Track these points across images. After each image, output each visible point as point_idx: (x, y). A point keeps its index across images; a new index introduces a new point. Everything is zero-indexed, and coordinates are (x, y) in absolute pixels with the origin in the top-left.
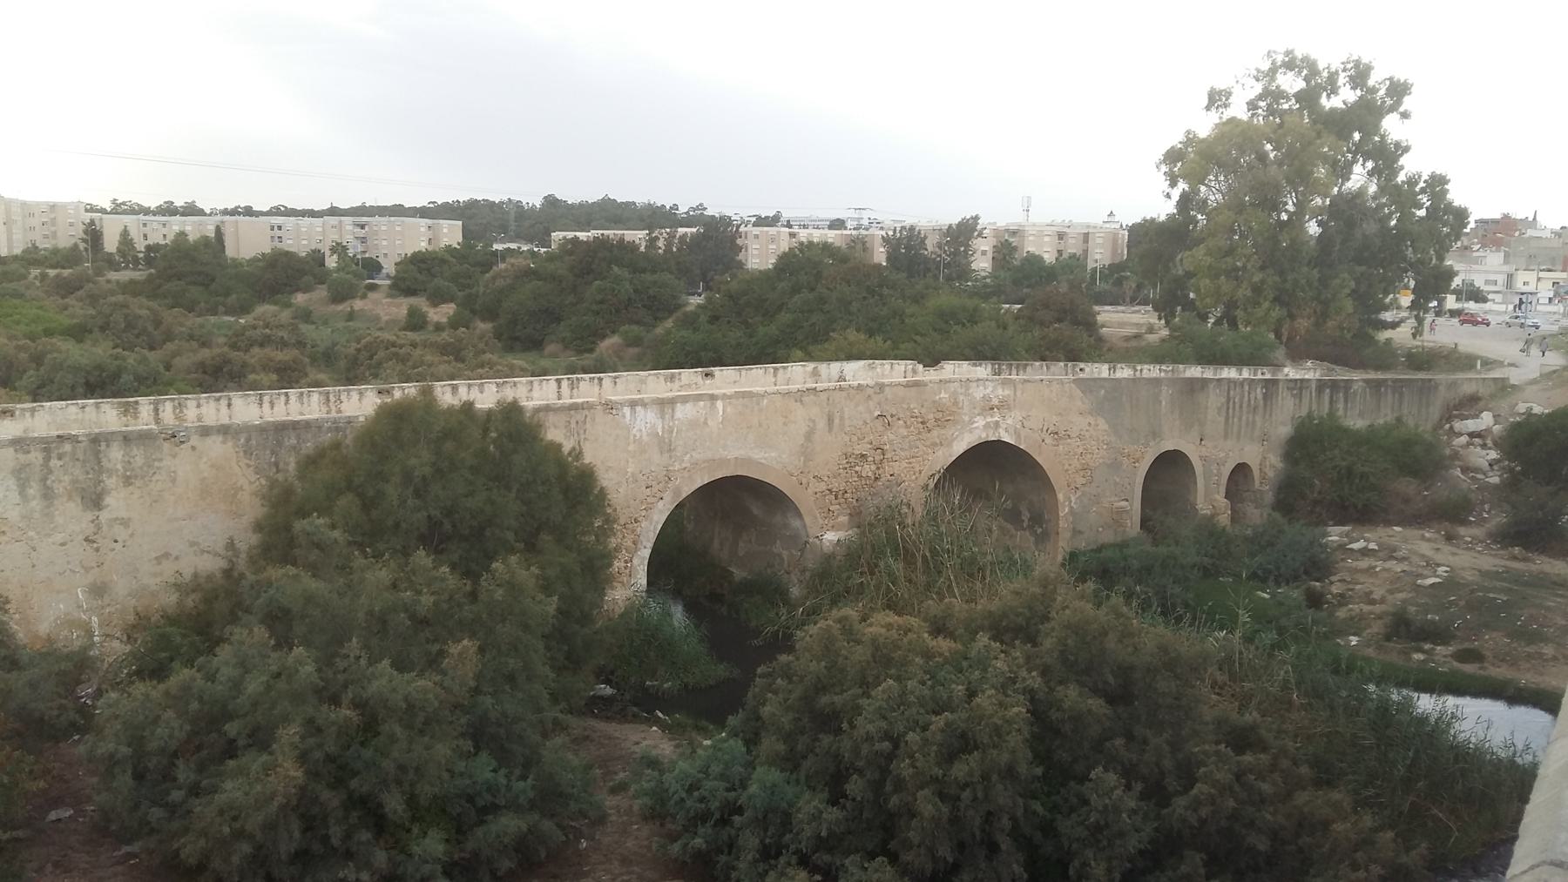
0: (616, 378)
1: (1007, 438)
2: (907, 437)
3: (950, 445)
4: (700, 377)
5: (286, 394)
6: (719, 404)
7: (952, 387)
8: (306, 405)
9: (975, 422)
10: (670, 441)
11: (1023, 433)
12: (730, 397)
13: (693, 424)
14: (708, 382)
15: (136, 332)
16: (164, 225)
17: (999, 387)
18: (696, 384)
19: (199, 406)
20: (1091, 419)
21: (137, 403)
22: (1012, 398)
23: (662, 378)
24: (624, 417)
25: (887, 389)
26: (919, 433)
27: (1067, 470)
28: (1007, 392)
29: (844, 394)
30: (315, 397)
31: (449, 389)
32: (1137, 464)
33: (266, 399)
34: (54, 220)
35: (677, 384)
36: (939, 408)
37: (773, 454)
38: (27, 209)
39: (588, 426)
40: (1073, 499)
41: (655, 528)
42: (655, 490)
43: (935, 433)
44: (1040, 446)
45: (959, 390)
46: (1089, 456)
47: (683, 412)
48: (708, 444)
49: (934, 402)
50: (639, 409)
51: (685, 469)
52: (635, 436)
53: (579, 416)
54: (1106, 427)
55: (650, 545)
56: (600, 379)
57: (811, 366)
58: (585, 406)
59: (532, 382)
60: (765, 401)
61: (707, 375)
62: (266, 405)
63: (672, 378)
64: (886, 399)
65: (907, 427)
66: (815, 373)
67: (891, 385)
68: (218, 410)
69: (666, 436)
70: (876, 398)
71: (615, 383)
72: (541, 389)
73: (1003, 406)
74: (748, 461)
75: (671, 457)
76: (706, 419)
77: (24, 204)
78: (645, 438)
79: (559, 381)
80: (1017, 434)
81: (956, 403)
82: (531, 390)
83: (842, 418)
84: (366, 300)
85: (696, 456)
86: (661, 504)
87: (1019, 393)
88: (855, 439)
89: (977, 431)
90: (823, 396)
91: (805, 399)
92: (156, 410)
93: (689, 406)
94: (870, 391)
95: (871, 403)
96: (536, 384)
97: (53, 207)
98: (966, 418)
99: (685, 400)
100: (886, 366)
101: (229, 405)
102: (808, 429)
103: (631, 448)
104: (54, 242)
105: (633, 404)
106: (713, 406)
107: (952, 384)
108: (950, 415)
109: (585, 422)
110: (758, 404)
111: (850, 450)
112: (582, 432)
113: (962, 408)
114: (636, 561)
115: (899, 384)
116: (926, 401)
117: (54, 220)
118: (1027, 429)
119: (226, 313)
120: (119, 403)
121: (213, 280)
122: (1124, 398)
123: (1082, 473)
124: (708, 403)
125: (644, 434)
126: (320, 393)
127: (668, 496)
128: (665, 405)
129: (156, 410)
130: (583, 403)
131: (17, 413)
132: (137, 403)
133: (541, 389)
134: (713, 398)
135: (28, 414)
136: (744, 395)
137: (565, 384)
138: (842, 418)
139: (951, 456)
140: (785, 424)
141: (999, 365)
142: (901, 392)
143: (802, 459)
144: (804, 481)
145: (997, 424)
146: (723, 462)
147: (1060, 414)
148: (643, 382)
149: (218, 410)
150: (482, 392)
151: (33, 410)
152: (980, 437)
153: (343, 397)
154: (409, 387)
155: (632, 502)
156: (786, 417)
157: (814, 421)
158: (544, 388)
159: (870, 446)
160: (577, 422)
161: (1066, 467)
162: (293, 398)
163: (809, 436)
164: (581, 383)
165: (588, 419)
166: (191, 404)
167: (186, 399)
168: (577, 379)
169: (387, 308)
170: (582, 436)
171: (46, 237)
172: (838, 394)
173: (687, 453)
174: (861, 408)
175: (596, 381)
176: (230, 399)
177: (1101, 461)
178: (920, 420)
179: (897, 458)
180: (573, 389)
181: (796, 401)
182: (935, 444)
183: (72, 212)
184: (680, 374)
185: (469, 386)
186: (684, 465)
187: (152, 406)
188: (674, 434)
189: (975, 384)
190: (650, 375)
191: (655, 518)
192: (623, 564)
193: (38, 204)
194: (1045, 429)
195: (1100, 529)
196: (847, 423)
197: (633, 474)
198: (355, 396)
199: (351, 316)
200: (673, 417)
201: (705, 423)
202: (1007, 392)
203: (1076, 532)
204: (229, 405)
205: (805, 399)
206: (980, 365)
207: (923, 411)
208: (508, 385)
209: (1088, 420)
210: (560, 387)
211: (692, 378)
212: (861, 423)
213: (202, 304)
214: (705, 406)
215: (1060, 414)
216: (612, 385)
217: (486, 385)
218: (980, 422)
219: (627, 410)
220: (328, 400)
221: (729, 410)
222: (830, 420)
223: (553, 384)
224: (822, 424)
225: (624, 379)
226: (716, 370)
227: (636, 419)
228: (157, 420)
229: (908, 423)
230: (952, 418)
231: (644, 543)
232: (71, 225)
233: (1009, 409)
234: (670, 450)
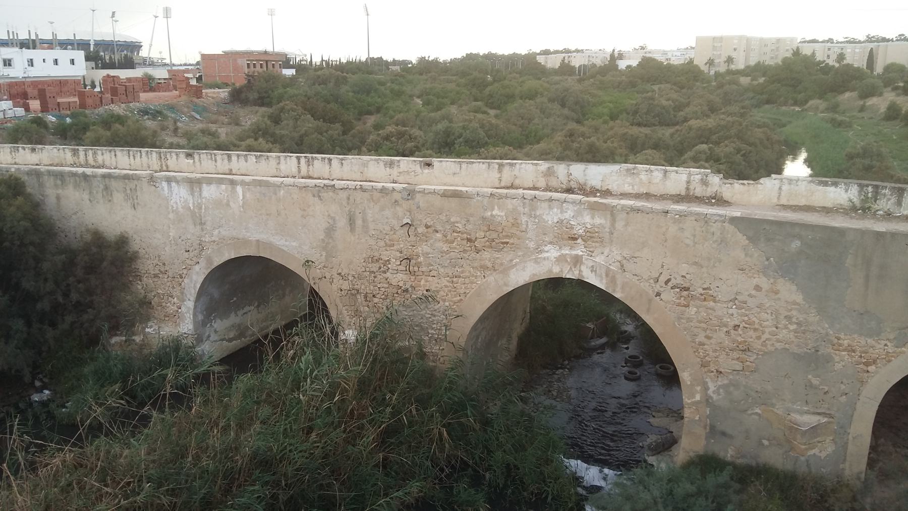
0: (342, 159)
1: (592, 279)
2: (447, 252)
3: (505, 271)
4: (418, 166)
5: (141, 152)
6: (239, 189)
7: (510, 204)
8: (150, 159)
9: (541, 252)
10: (200, 215)
11: (619, 280)
12: (248, 184)
13: (219, 204)
14: (427, 171)
15: (653, 115)
16: (842, 49)
17: (585, 213)
18: (414, 171)
19: (102, 154)
20: (764, 283)
21: (78, 149)
22: (607, 230)
23: (382, 164)
24: (163, 189)
25: (418, 196)
26: (465, 251)
27: (702, 344)
28: (598, 221)
29: (366, 195)
30: (154, 155)
31: (226, 157)
32: (872, 368)
33: (131, 153)
34: (777, 48)
35: (395, 172)
36: (489, 225)
37: (294, 244)
38: (763, 43)
39: (139, 193)
40: (712, 387)
41: (195, 286)
42: (192, 254)
43: (486, 255)
44: (650, 301)
45: (521, 209)
46: (751, 333)
47: (210, 192)
48: (232, 223)
49: (484, 219)
50: (173, 184)
51: (214, 241)
52: (173, 207)
53: (132, 185)
54: (799, 298)
55: (193, 298)
56: (330, 160)
57: (543, 165)
58: (134, 178)
59: (279, 157)
60: (282, 192)
61: (429, 165)
62: (132, 157)
63: (391, 165)
64: (418, 207)
65: (447, 241)
66: (549, 173)
67: (423, 192)
68: (111, 158)
69: (196, 211)
70: (405, 205)
71: (342, 164)
72: (286, 163)
73: (591, 237)
74: (270, 246)
75: (202, 230)
76: (228, 201)
77: (761, 40)
78: (180, 209)
79: (298, 158)
80: (613, 280)
81: (516, 224)
82: (279, 163)
83: (364, 221)
84: (879, 98)
85: (224, 233)
86: (197, 268)
87: (619, 225)
88: (382, 243)
89: (546, 263)
90: (343, 195)
91: (324, 195)
92: (86, 155)
93: (213, 187)
94: (397, 196)
95: (398, 208)
96: (282, 159)
97: (778, 40)
98: (532, 245)
99: (209, 181)
100: (656, 174)
101: (115, 155)
102: (328, 225)
103: (171, 216)
104: (776, 61)
105: (169, 180)
106: (234, 191)
107: (508, 201)
108: (507, 236)
109: (136, 190)
110: (276, 194)
111: (376, 254)
112: (135, 197)
113: (525, 231)
114: (183, 309)
115: (434, 192)
116: (472, 215)
117: (777, 48)
118: (628, 275)
119: (796, 103)
120: (72, 149)
121: (800, 83)
122: (849, 261)
123: (736, 355)
124: (229, 187)
125: (180, 207)
126: (156, 152)
127: (203, 262)
128: (194, 184)
129: (86, 155)
130: (132, 175)
131: (37, 150)
132: (78, 149)
133: (286, 163)
134: (233, 183)
135: (40, 151)
136: (260, 183)
137: (303, 161)
138: (364, 221)
139: (506, 285)
140: (304, 217)
141: (876, 187)
142: (438, 201)
143: (324, 254)
144: (328, 275)
145: (577, 260)
146: (246, 242)
147: (696, 263)
148: (365, 165)
149: (111, 158)
150: (246, 162)
151: (42, 149)
152: (550, 271)
153: (168, 156)
154: (203, 153)
155: (176, 260)
156: (304, 210)
157: (334, 219)
158: (289, 163)
159: (398, 254)
160: (131, 189)
161: (701, 338)
162: (144, 154)
163: (330, 231)
164: (316, 162)
165: (138, 188)
166: (99, 153)
167: (97, 149)
168: (312, 158)
169: (880, 103)
170: (136, 201)
171: (772, 58)
172: (359, 195)
173: (214, 229)
174: (388, 213)
175: (326, 161)
176: (115, 152)
177: (778, 345)
178: (465, 236)
179: (433, 273)
180: (309, 165)
181: (314, 196)
182: (484, 268)
183: (788, 42)
184: (399, 161)
185: (238, 156)
186: (213, 239)
187: (84, 152)
188: (203, 211)
189: (545, 205)
190: (372, 160)
191: (194, 277)
192: (177, 309)
193: (770, 39)
194: (663, 279)
195: (766, 442)
196: (372, 226)
197: (174, 238)
198: (174, 157)
199: (862, 109)
200: (200, 195)
201: (228, 205)
202: (598, 221)
203: (713, 432)
204: (115, 155)
205: (324, 195)
206: (835, 184)
207: (470, 227)
208: (263, 158)
209: (755, 281)
210: (299, 163)
211: (411, 166)
212: (387, 228)
213: (782, 99)
214: (226, 188)
215: (696, 263)
216: (339, 166)
217: (249, 156)
218: (552, 252)
219: (165, 184)
220: (161, 158)
221: (248, 195)
222: (351, 221)
223: (294, 160)
224: (342, 222)
225: (349, 161)
226: (435, 161)
227: (172, 193)
228: (95, 161)
229: (449, 237)
230: (511, 241)
231: (188, 296)
232: (787, 50)
233: (602, 241)
234: (201, 224)
